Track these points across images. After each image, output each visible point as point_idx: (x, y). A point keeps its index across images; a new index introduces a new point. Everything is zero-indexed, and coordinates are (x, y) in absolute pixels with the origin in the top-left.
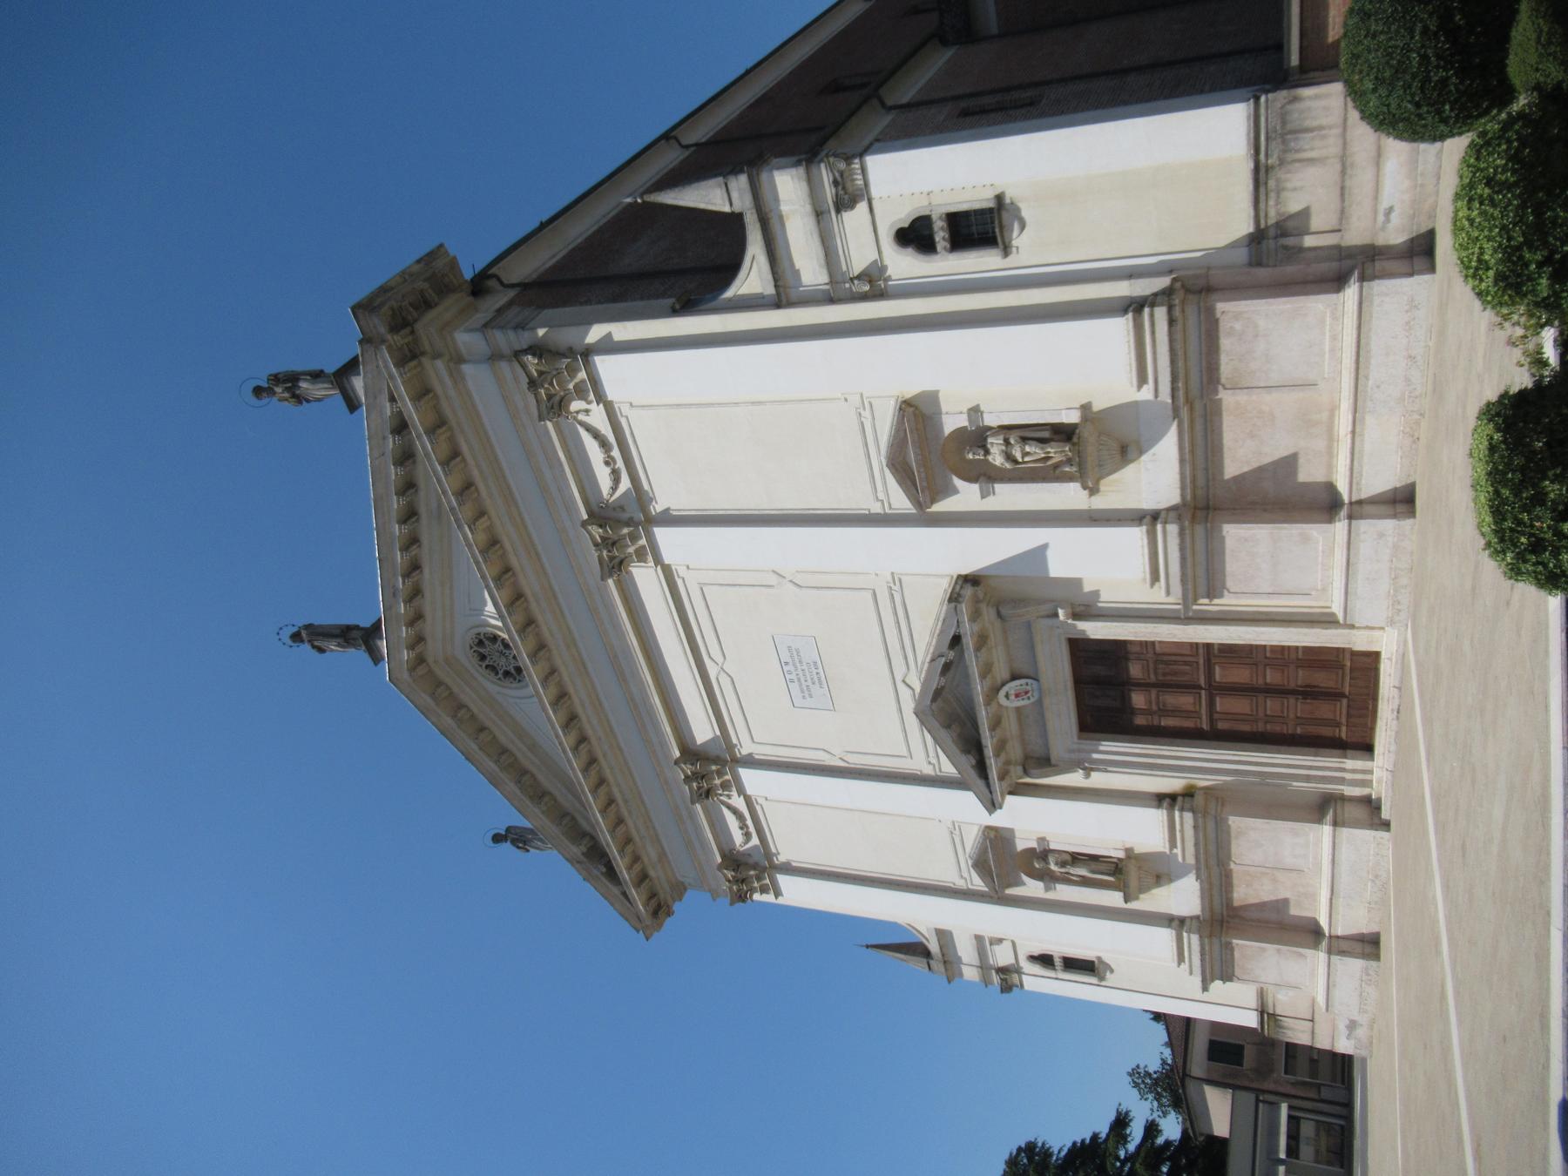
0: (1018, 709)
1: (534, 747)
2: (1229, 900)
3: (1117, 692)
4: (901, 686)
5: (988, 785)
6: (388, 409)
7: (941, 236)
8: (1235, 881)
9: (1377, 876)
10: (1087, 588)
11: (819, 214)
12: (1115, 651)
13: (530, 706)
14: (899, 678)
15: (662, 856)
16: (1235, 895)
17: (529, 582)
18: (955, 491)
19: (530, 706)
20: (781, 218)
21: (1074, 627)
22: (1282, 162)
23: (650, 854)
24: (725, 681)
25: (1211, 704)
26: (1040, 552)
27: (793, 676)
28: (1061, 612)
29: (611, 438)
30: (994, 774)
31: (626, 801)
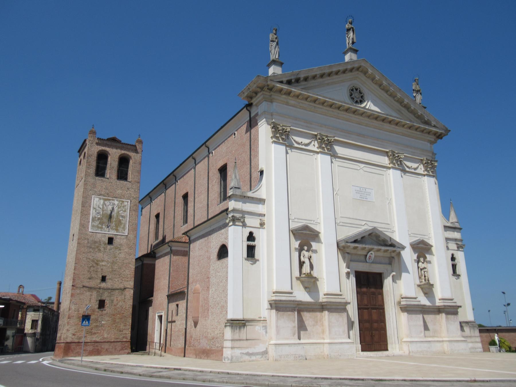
0: (366, 256)
1: (328, 84)
2: (303, 311)
3: (369, 285)
4: (365, 222)
5: (352, 242)
6: (433, 123)
7: (453, 262)
8: (311, 313)
9: (340, 356)
10: (397, 281)
11: (456, 240)
12: (380, 286)
13: (338, 93)
14: (367, 223)
15: (287, 104)
16: (305, 313)
17: (386, 126)
18: (415, 254)
19: (338, 93)
20: (454, 231)
21: (389, 276)
22: (470, 327)
23: (292, 101)
24: (355, 167)
25: (366, 309)
26: (407, 271)
27: (362, 190)
28: (394, 273)
29: (416, 171)
30: (356, 245)
31: (315, 107)
